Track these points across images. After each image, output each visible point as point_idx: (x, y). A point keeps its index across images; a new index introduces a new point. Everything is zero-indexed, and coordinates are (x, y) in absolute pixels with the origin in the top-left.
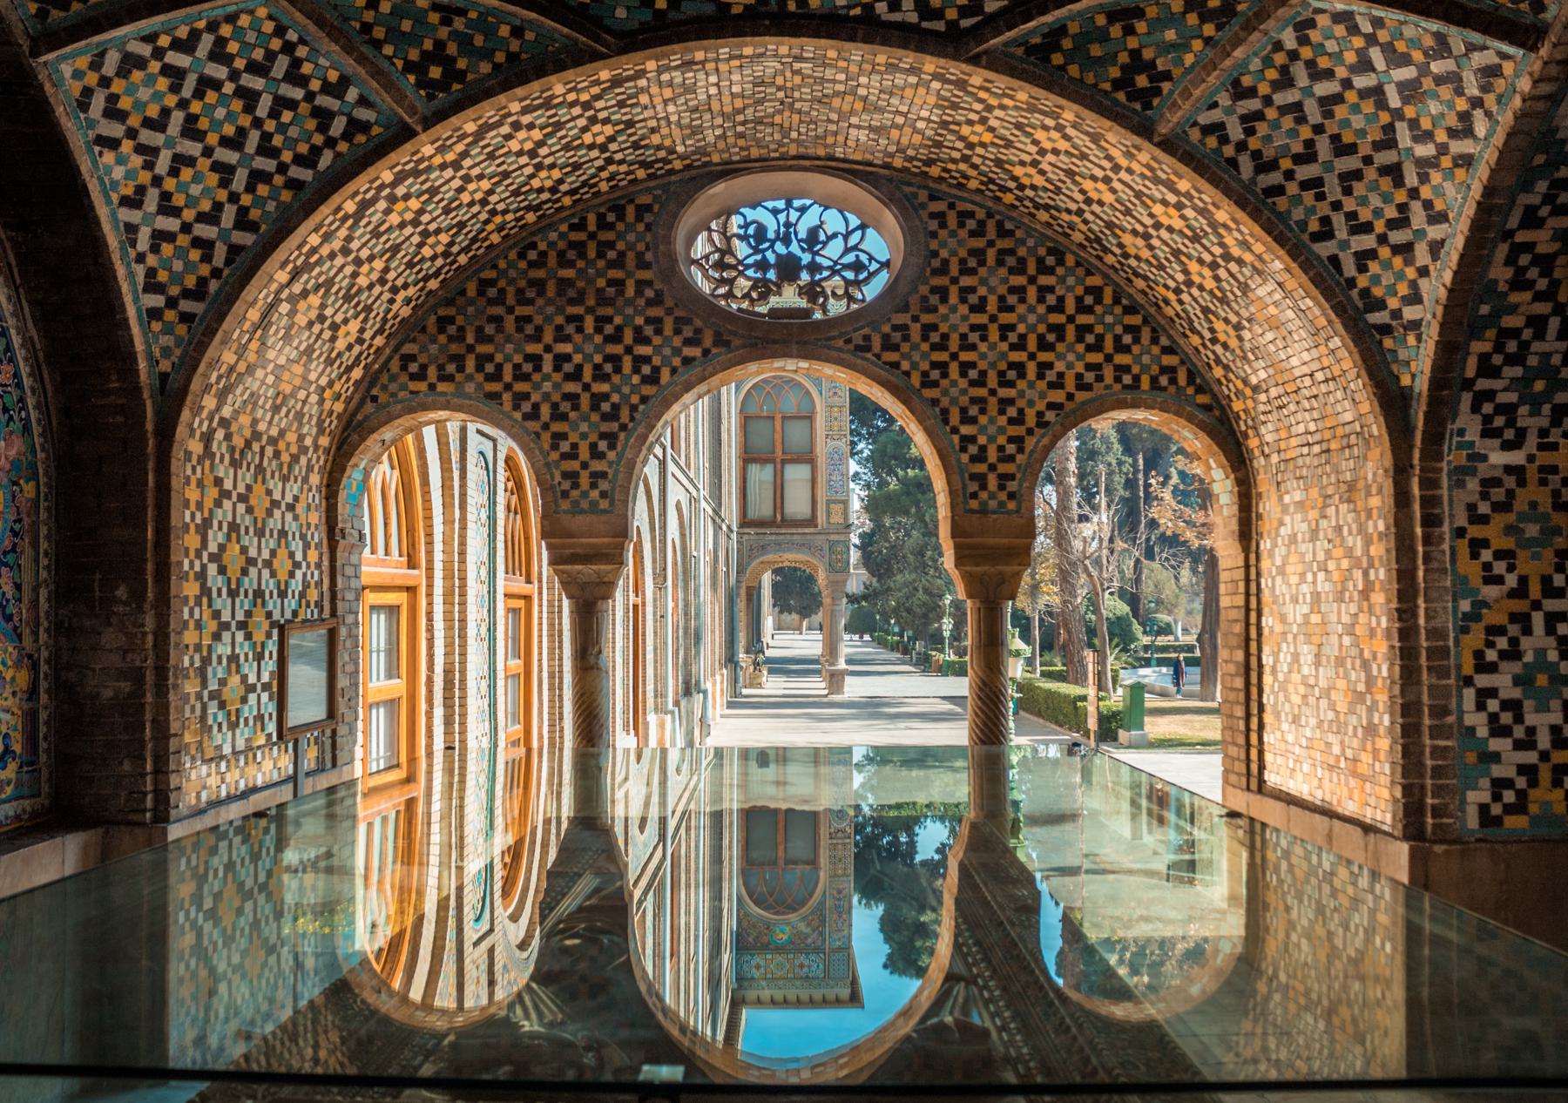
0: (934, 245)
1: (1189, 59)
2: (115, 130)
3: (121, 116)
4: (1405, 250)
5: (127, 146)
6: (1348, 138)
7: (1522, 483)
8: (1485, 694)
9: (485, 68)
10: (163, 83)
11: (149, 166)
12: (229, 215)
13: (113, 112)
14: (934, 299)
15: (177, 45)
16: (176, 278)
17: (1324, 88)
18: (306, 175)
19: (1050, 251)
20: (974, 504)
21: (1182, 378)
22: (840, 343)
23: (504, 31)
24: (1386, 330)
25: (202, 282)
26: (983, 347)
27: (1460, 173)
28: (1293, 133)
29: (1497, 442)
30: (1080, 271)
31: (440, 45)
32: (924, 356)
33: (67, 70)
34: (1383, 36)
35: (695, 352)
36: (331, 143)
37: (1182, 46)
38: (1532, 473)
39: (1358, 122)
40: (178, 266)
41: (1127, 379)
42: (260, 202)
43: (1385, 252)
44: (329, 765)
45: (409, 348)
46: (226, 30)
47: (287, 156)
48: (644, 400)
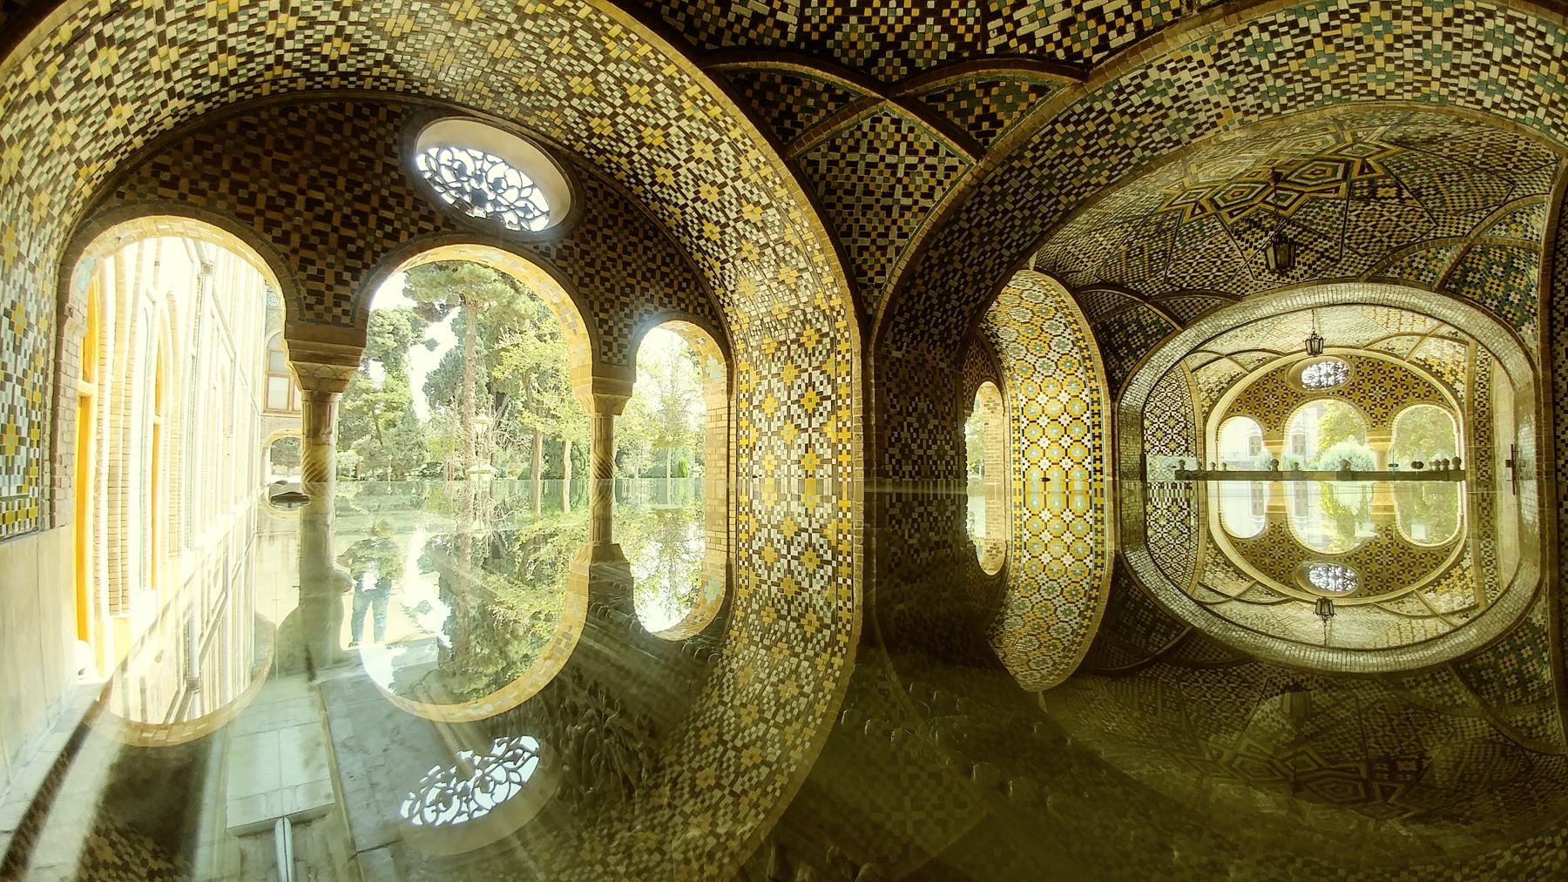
0: (590, 206)
1: (815, 119)
4: (883, 249)
6: (872, 187)
8: (892, 456)
14: (589, 237)
17: (871, 158)
19: (651, 228)
20: (605, 358)
21: (707, 312)
22: (531, 247)
24: (864, 286)
26: (614, 271)
27: (921, 216)
28: (848, 178)
30: (665, 244)
32: (581, 268)
34: (911, 137)
37: (815, 111)
39: (879, 179)
41: (683, 306)
43: (873, 248)
44: (47, 525)
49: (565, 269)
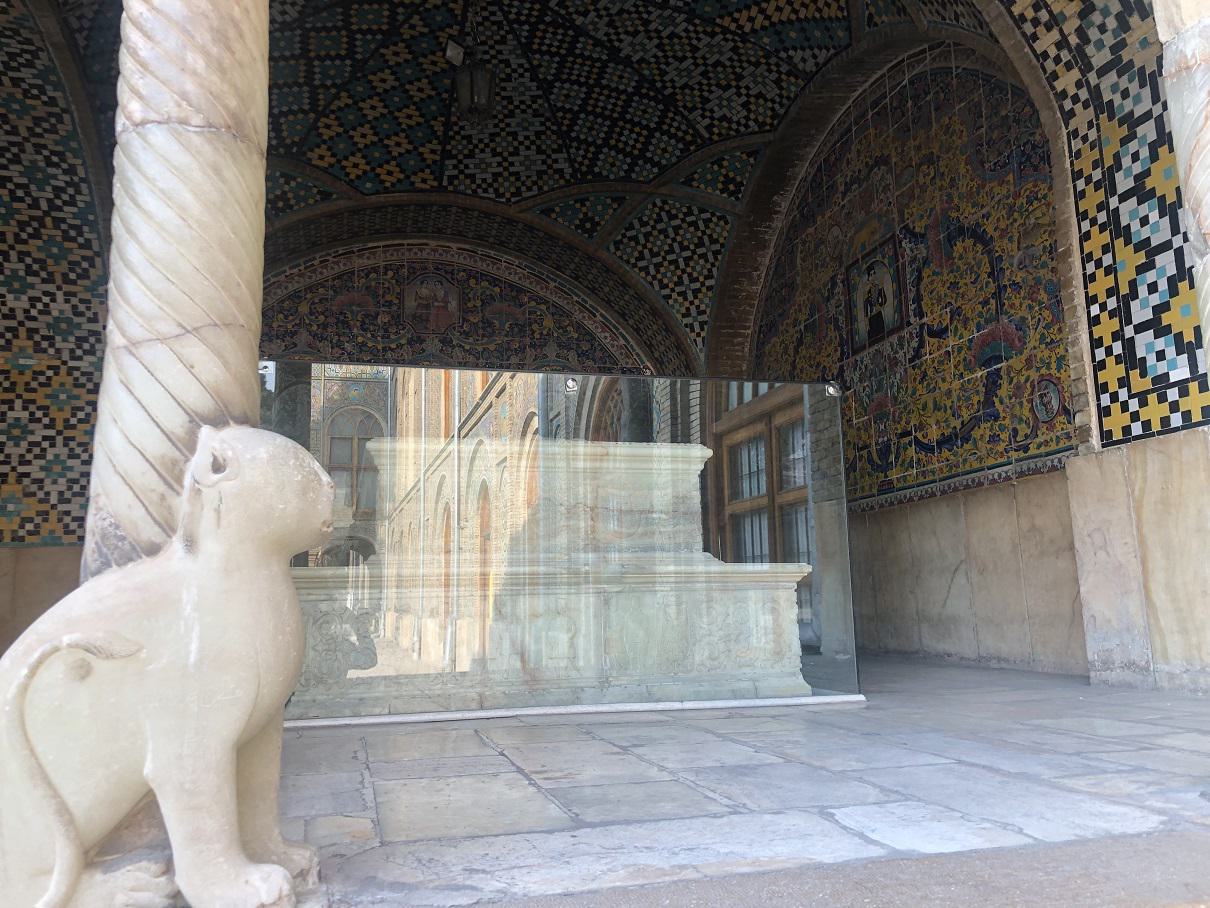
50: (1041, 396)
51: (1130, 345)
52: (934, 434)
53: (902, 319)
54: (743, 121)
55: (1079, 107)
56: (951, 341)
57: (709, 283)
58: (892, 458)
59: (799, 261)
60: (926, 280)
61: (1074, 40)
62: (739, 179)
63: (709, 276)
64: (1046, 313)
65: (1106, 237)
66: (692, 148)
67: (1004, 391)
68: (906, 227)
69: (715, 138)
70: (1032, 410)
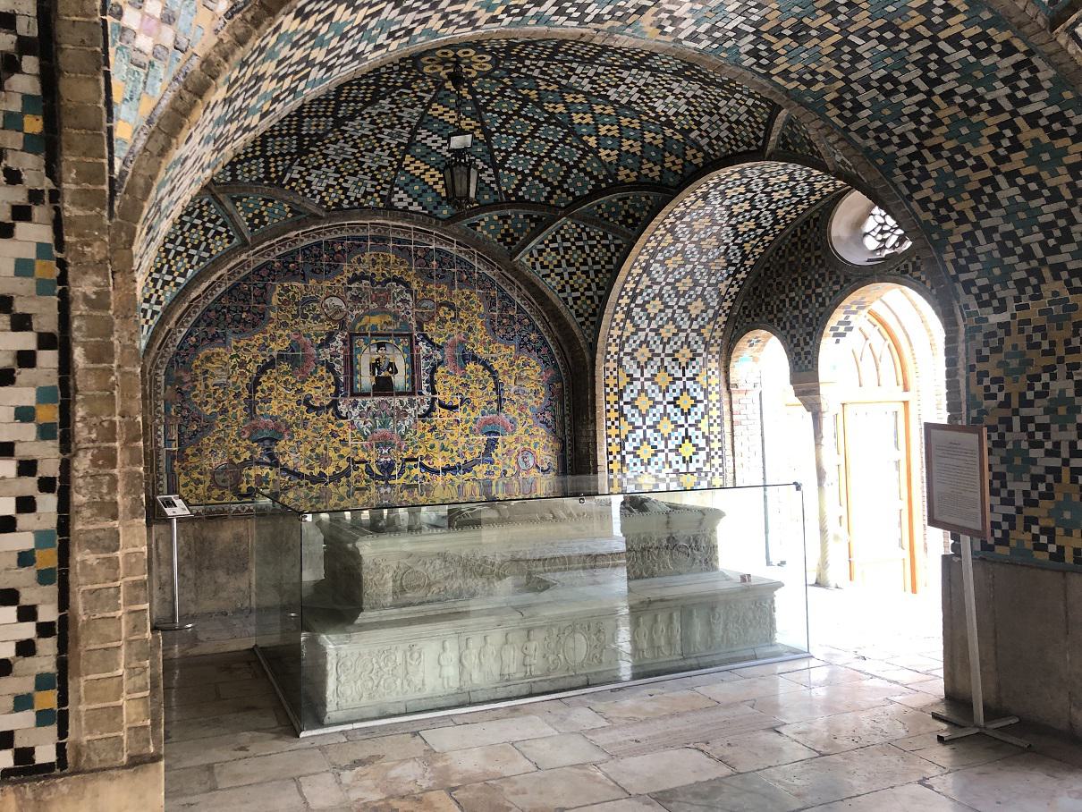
2: (547, 271)
3: (547, 267)
5: (553, 275)
7: (1008, 333)
9: (645, 214)
10: (553, 254)
11: (562, 278)
12: (594, 286)
13: (544, 267)
15: (551, 242)
16: (586, 311)
18: (611, 267)
23: (643, 199)
25: (594, 310)
29: (990, 309)
31: (627, 211)
33: (524, 260)
35: (837, 287)
36: (613, 254)
38: (1014, 328)
40: (585, 307)
42: (601, 280)
45: (746, 304)
46: (562, 232)
47: (603, 263)
48: (821, 314)
49: (919, 278)
50: (523, 458)
51: (623, 457)
52: (439, 463)
53: (414, 389)
54: (315, 192)
55: (612, 360)
56: (460, 415)
57: (180, 280)
58: (395, 472)
59: (275, 300)
60: (439, 373)
61: (624, 339)
62: (266, 219)
63: (183, 275)
64: (529, 420)
65: (617, 415)
66: (266, 182)
67: (500, 450)
68: (425, 337)
69: (287, 187)
70: (517, 463)
